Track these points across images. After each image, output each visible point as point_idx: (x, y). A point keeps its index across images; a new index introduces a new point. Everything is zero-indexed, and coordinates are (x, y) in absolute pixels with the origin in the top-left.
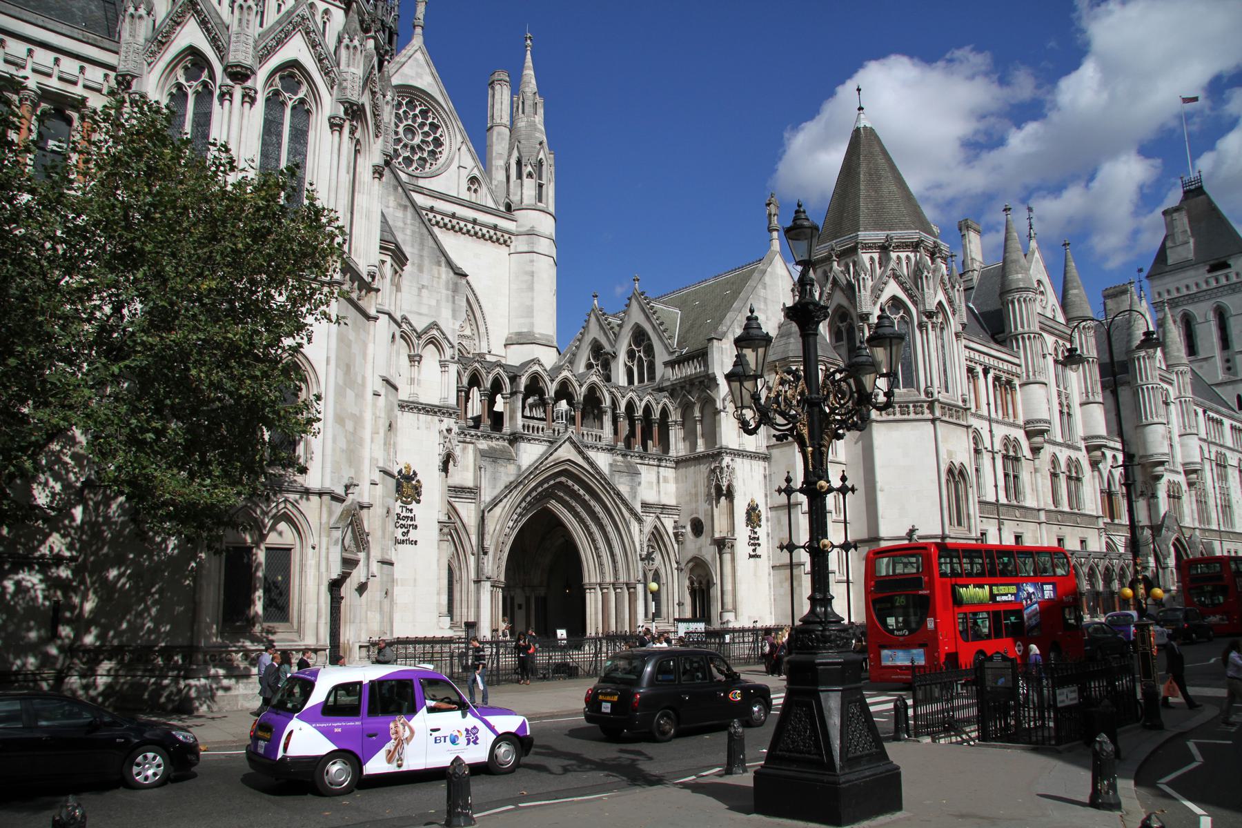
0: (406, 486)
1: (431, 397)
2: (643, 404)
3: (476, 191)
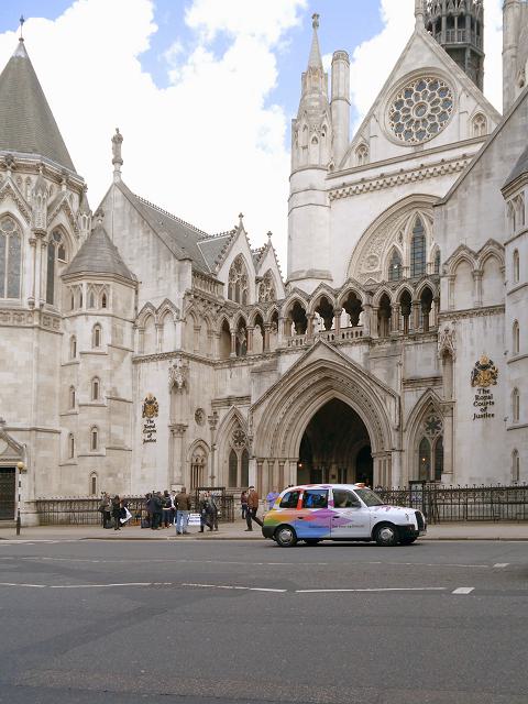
0: (150, 407)
1: (167, 349)
2: (420, 286)
3: (483, 125)
